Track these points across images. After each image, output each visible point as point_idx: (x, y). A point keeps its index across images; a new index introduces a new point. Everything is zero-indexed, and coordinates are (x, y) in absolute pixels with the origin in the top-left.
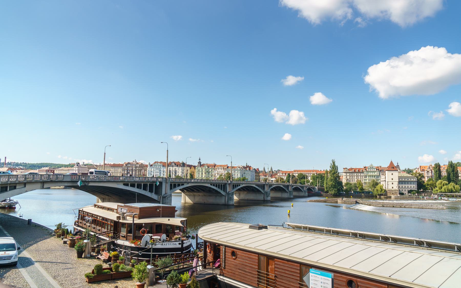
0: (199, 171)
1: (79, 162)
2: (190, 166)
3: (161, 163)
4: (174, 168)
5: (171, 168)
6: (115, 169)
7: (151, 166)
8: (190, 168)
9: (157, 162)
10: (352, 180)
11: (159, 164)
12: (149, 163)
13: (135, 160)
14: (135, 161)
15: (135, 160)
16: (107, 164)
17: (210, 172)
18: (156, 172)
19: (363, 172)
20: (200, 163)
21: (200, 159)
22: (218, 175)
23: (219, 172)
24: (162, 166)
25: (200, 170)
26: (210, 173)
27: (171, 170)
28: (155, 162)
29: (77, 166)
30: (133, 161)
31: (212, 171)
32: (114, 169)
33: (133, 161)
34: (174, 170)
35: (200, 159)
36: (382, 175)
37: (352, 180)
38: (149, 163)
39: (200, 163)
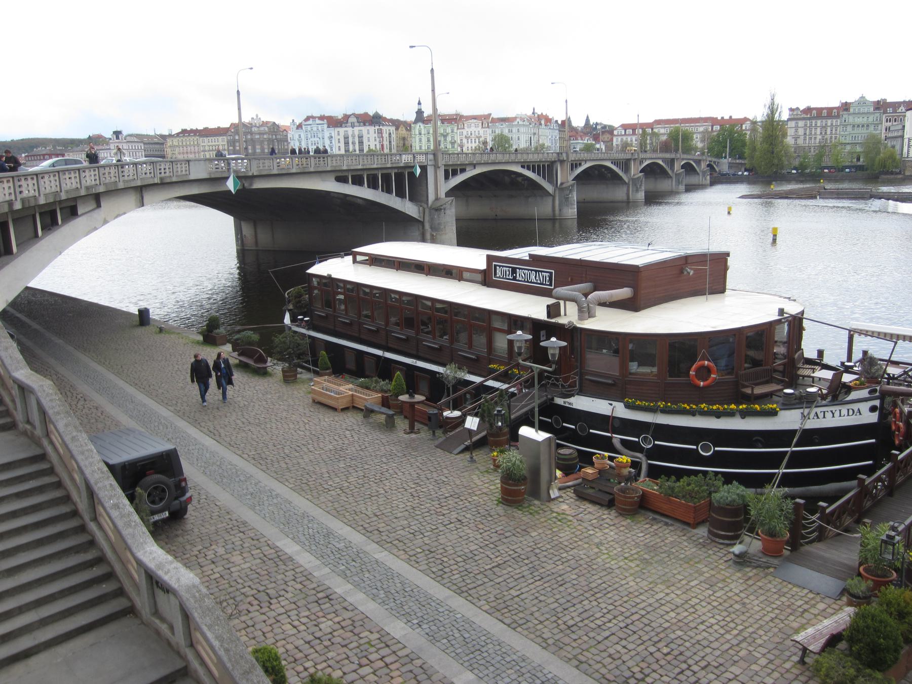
0: (420, 134)
1: (119, 130)
2: (396, 124)
3: (322, 118)
4: (356, 129)
5: (350, 130)
7: (300, 127)
8: (397, 129)
9: (313, 117)
10: (810, 139)
11: (318, 121)
12: (293, 121)
13: (257, 116)
14: (255, 118)
15: (257, 116)
16: (189, 129)
17: (448, 134)
18: (312, 144)
19: (838, 117)
20: (420, 113)
21: (419, 103)
22: (468, 142)
23: (471, 134)
24: (326, 126)
25: (423, 132)
26: (449, 139)
27: (350, 133)
28: (308, 119)
30: (252, 118)
31: (452, 131)
33: (252, 118)
34: (357, 133)
35: (419, 103)
36: (887, 121)
37: (810, 139)
38: (293, 121)
39: (420, 113)
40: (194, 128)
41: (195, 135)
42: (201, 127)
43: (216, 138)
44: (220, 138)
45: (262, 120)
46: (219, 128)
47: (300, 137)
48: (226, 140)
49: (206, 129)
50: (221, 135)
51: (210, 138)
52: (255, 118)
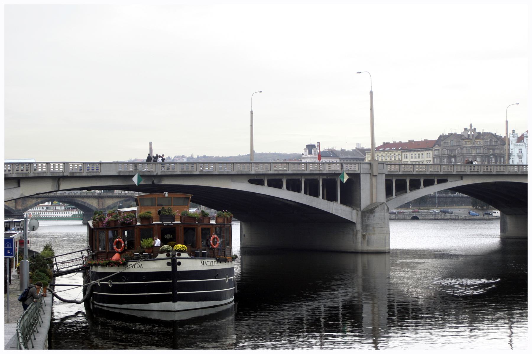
6: (414, 156)
13: (471, 126)
15: (471, 126)
16: (391, 142)
29: (309, 156)
30: (466, 129)
32: (412, 158)
33: (466, 129)
40: (398, 141)
41: (397, 150)
42: (405, 140)
43: (420, 153)
44: (425, 153)
45: (477, 131)
46: (426, 141)
47: (521, 152)
48: (431, 155)
49: (411, 142)
50: (426, 149)
51: (414, 153)
52: (469, 128)
